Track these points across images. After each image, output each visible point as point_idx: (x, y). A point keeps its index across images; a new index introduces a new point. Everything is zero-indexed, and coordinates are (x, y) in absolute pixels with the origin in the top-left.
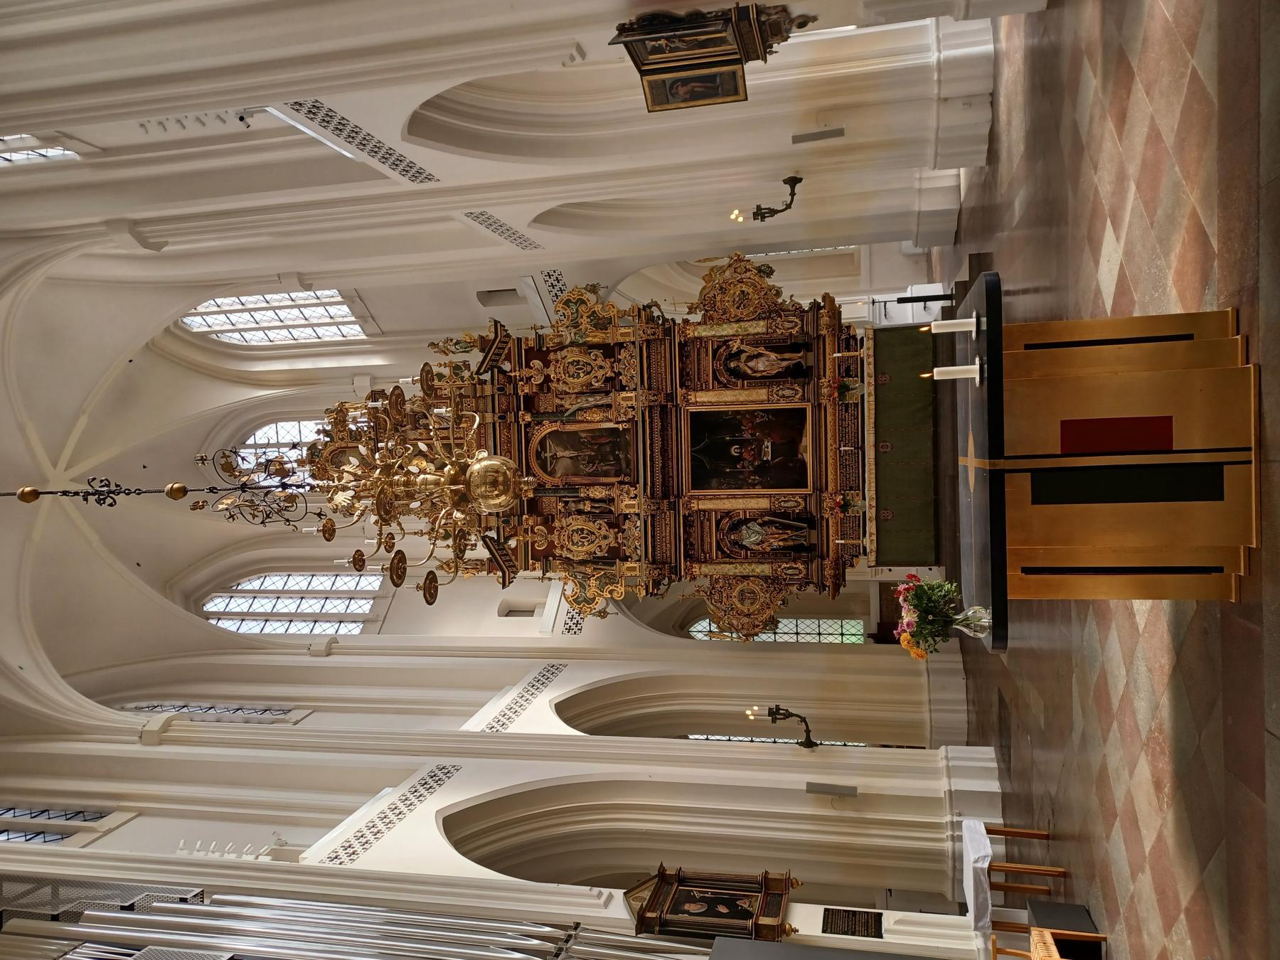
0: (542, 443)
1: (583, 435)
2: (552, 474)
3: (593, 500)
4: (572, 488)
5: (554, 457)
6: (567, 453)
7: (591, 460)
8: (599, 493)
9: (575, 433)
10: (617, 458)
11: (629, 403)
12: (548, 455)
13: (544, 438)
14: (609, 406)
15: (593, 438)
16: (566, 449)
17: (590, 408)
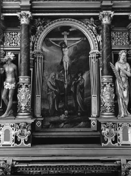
0: (78, 33)
1: (85, 76)
2: (46, 42)
3: (16, 92)
4: (30, 64)
5: (63, 46)
6: (66, 60)
7: (59, 84)
8: (24, 96)
9: (87, 68)
10: (60, 112)
11: (121, 137)
12: (66, 39)
13: (82, 35)
14: (116, 111)
15: (82, 87)
16: (71, 58)
17: (115, 92)
